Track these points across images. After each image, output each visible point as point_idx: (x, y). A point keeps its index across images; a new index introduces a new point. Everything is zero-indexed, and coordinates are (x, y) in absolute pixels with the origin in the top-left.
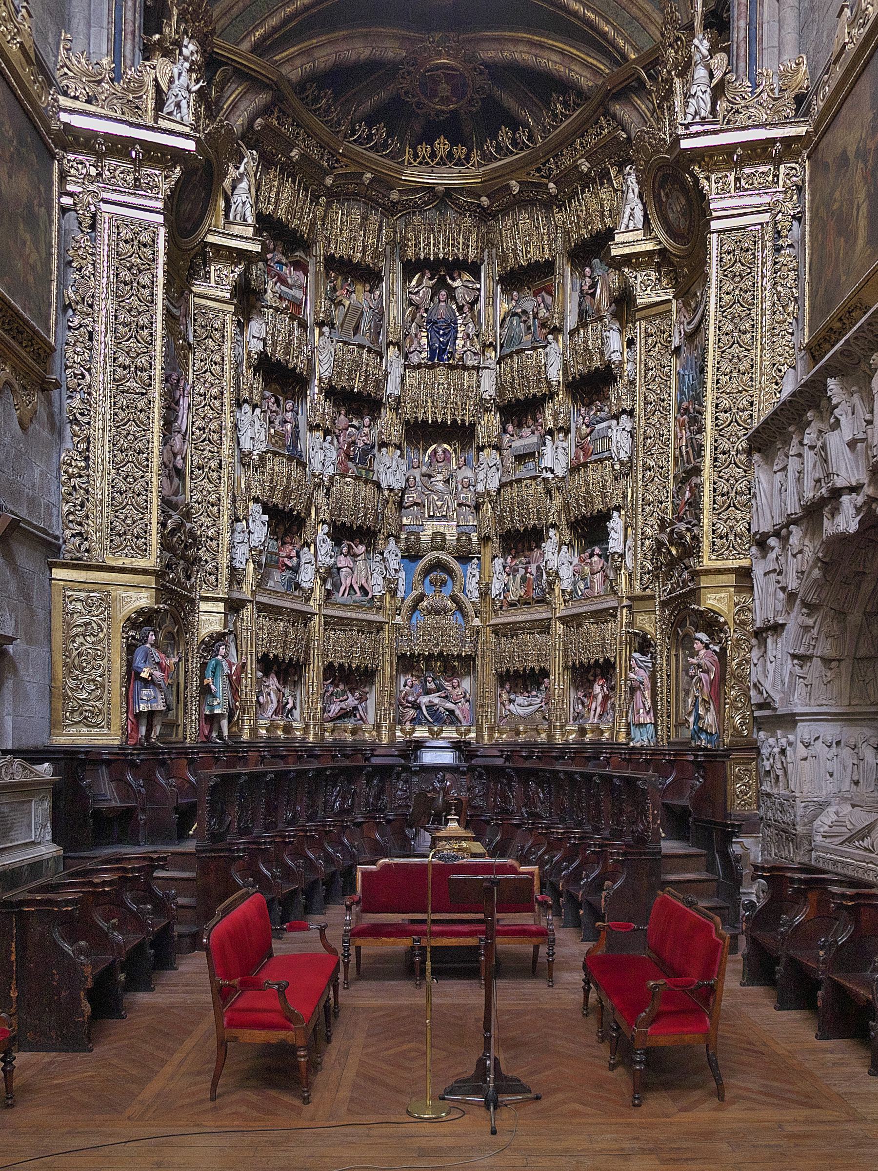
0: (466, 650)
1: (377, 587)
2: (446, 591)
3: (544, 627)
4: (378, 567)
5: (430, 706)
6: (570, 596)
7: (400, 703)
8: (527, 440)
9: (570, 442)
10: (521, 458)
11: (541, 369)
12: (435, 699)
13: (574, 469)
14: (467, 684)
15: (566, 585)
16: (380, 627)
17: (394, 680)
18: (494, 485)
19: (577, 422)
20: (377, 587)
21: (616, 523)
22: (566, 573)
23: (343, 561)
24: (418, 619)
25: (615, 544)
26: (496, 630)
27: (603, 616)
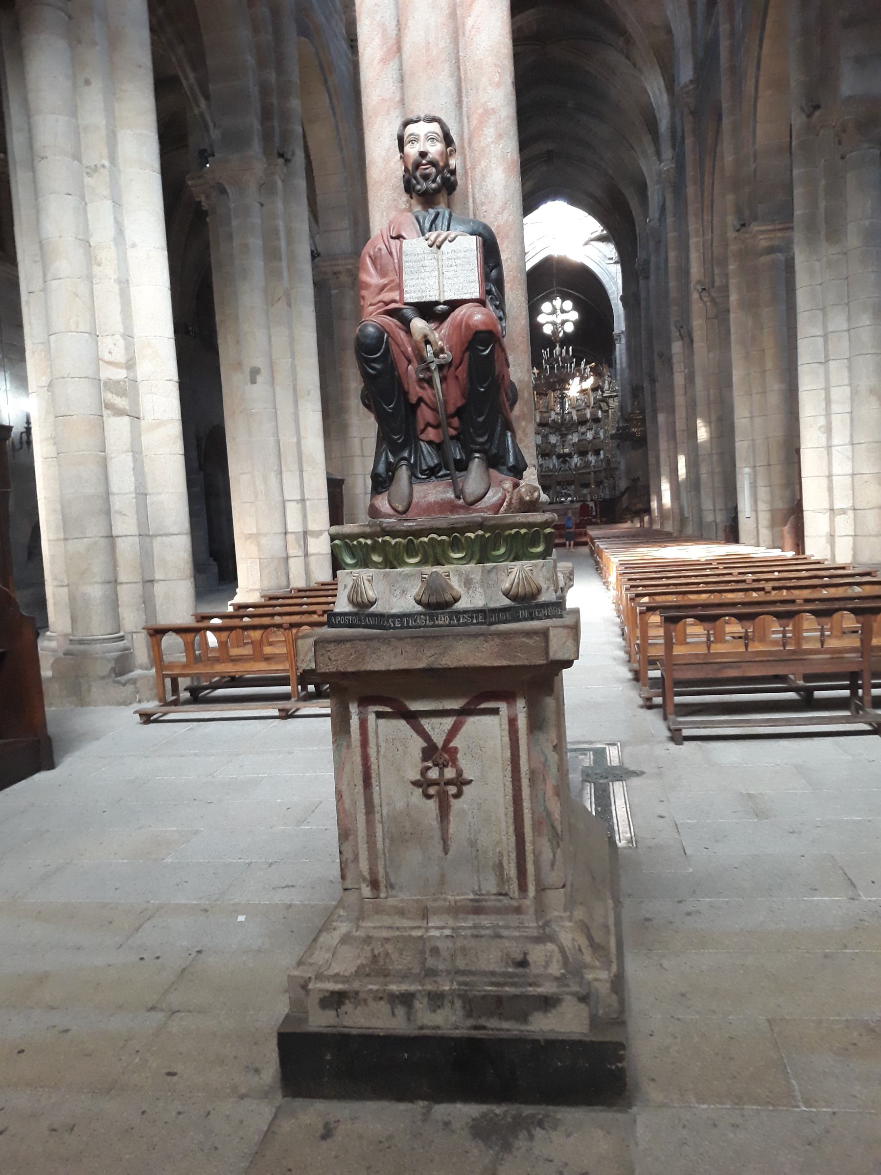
0: (572, 479)
1: (551, 467)
2: (567, 465)
3: (589, 473)
4: (551, 462)
5: (565, 493)
6: (594, 466)
7: (558, 492)
8: (582, 429)
9: (593, 431)
10: (583, 434)
11: (585, 415)
12: (566, 491)
13: (594, 438)
14: (573, 487)
15: (593, 464)
16: (551, 476)
17: (556, 487)
18: (577, 440)
19: (594, 426)
20: (551, 467)
21: (602, 452)
22: (593, 461)
23: (543, 462)
24: (560, 472)
25: (602, 456)
26: (579, 474)
27: (600, 471)
